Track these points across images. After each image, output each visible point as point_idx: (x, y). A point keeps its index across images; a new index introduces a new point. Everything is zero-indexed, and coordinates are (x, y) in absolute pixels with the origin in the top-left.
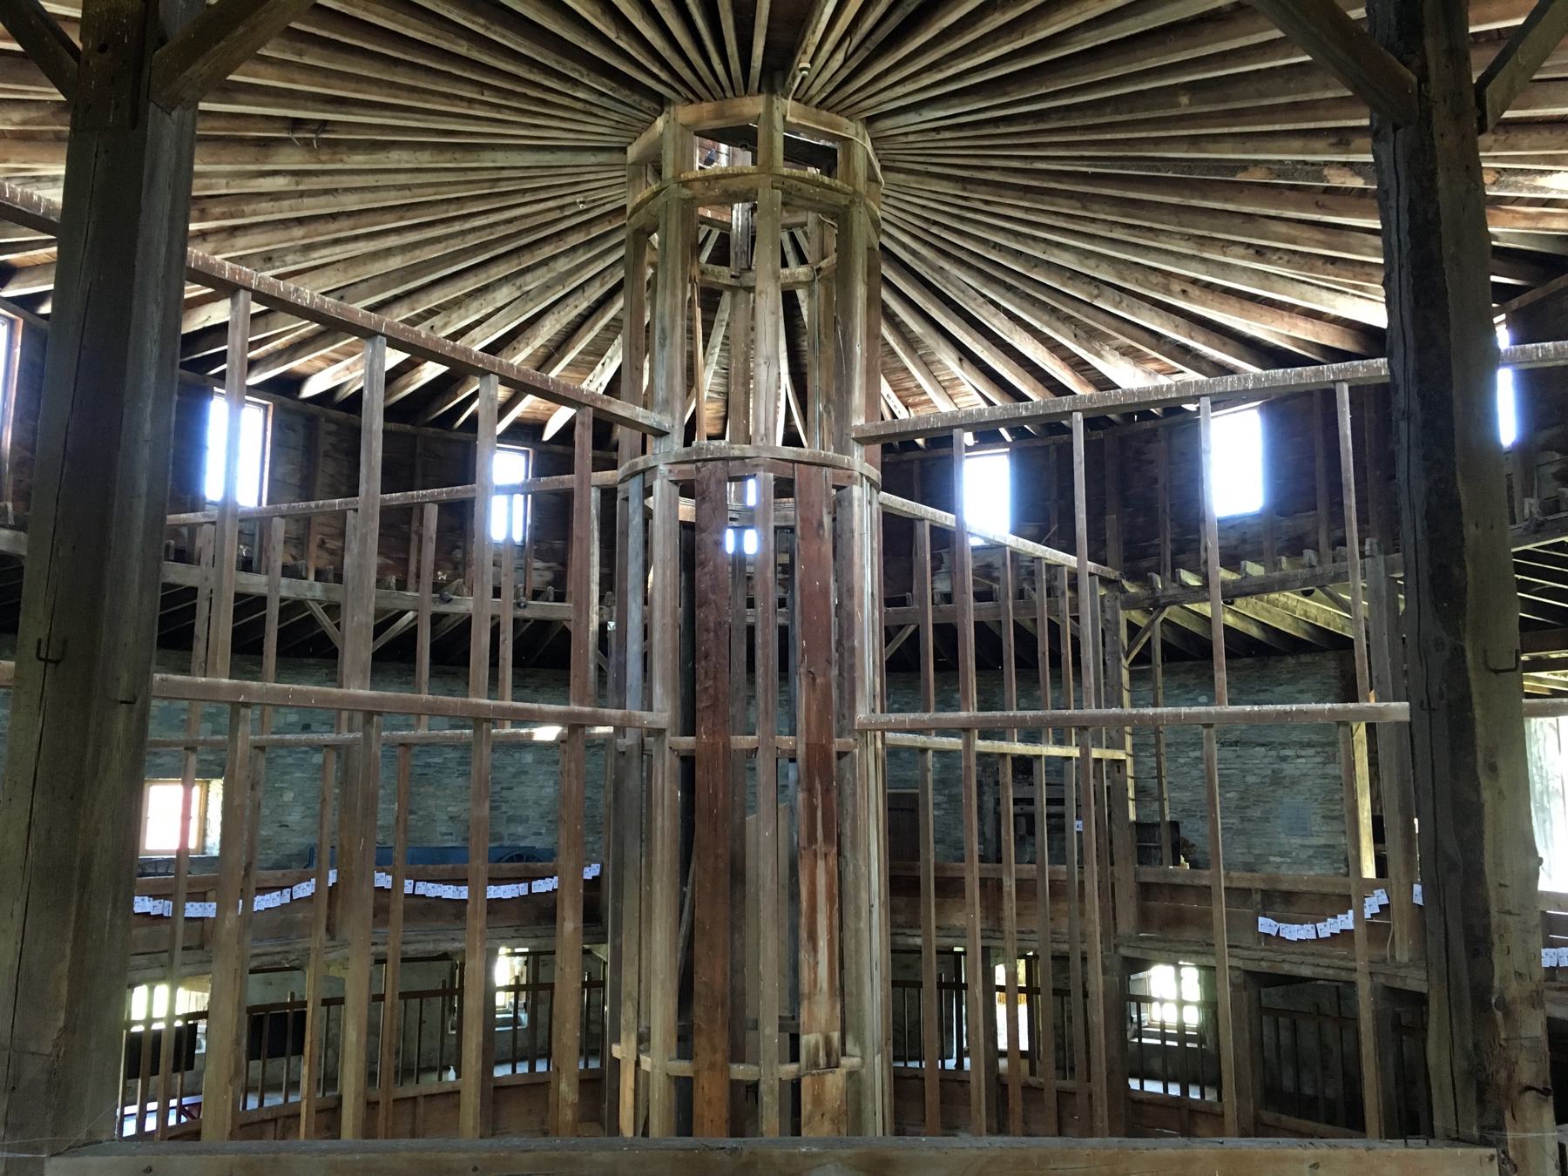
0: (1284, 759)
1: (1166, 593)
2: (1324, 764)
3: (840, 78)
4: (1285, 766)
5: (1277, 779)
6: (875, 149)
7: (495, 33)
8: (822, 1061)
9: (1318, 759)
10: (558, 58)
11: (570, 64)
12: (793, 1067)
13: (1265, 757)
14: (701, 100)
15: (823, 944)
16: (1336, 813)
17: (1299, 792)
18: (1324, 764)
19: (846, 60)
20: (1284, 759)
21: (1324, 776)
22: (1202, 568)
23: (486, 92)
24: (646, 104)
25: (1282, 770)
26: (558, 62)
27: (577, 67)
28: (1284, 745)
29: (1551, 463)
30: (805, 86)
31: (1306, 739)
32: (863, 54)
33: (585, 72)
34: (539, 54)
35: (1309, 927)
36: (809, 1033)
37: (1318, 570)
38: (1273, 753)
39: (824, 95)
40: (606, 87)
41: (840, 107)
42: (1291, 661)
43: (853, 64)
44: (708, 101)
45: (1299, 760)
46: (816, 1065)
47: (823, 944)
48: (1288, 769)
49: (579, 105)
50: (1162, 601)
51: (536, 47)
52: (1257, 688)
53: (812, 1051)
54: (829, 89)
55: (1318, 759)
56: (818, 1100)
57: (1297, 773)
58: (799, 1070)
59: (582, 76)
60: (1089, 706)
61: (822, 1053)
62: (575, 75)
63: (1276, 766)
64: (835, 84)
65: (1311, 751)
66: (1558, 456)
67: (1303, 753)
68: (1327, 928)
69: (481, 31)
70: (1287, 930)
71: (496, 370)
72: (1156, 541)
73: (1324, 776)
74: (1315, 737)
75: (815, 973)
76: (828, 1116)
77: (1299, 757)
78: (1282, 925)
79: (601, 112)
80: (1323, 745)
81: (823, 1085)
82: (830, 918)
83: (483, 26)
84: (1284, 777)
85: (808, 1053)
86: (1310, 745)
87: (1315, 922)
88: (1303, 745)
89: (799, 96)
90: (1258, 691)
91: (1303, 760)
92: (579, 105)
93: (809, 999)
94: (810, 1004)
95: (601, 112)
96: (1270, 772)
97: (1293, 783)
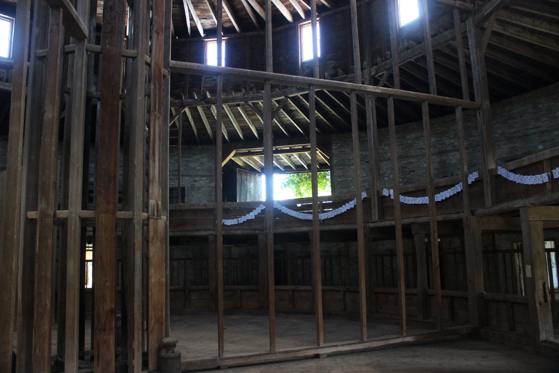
0: (195, 181)
1: (187, 101)
2: (209, 183)
4: (196, 183)
5: (193, 188)
8: (156, 214)
9: (209, 181)
12: (146, 214)
13: (189, 180)
15: (157, 159)
16: (212, 199)
17: (200, 192)
18: (209, 183)
20: (195, 181)
21: (209, 187)
22: (202, 93)
25: (194, 185)
28: (196, 176)
29: (331, 64)
31: (203, 174)
35: (235, 220)
36: (152, 199)
37: (246, 96)
38: (192, 179)
42: (200, 147)
45: (201, 181)
46: (154, 215)
47: (157, 159)
48: (197, 184)
50: (186, 104)
52: (187, 156)
53: (153, 208)
55: (207, 181)
56: (156, 231)
57: (200, 186)
58: (148, 216)
60: (271, 72)
61: (156, 211)
63: (193, 183)
65: (205, 178)
66: (333, 62)
67: (203, 179)
68: (242, 219)
70: (227, 222)
72: (183, 83)
73: (209, 187)
74: (206, 174)
75: (154, 172)
76: (159, 239)
77: (201, 180)
78: (225, 220)
80: (209, 176)
81: (157, 225)
82: (159, 148)
84: (195, 188)
85: (151, 208)
86: (205, 176)
87: (237, 218)
88: (202, 176)
90: (188, 157)
91: (202, 181)
93: (152, 183)
94: (152, 185)
96: (190, 186)
97: (198, 189)
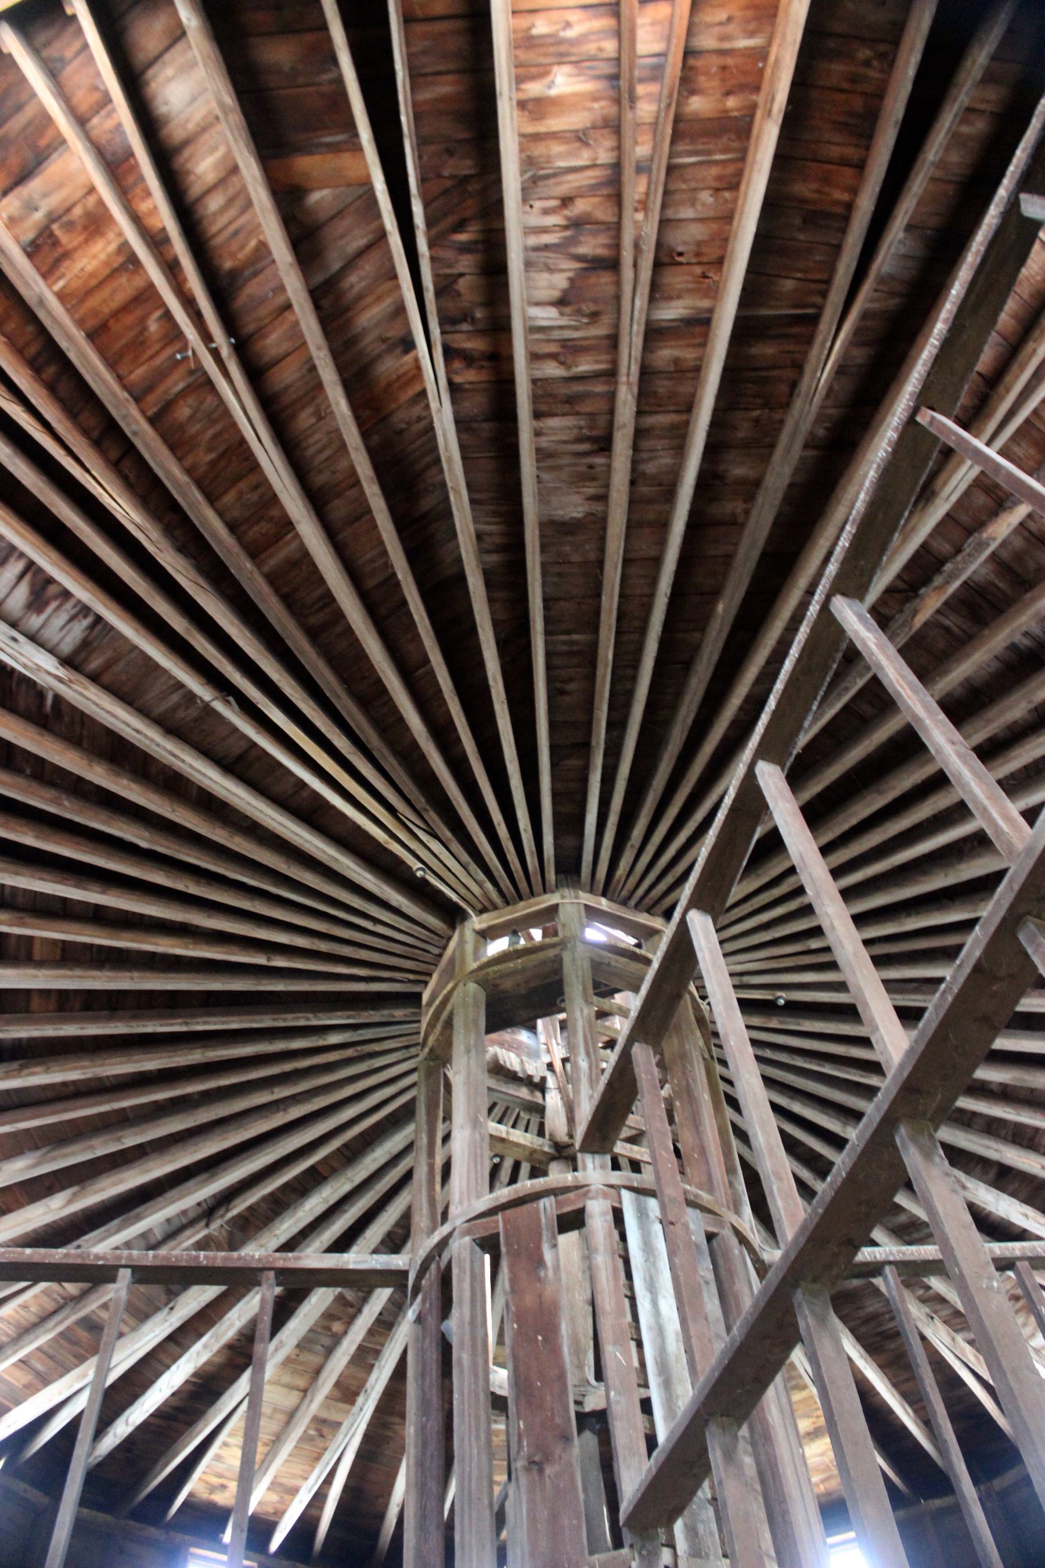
3: (465, 857)
6: (624, 903)
7: (197, 1023)
10: (275, 1017)
11: (290, 1016)
14: (430, 975)
19: (435, 836)
23: (276, 1090)
24: (399, 1014)
26: (274, 1020)
27: (300, 1015)
30: (463, 891)
32: (432, 817)
33: (310, 1015)
34: (250, 1021)
39: (488, 885)
40: (342, 1018)
41: (523, 885)
43: (446, 834)
44: (434, 971)
49: (350, 1053)
51: (244, 1018)
54: (481, 876)
59: (308, 1019)
62: (302, 1023)
64: (473, 867)
69: (184, 1029)
71: (123, 1262)
79: (376, 1047)
83: (181, 1024)
89: (479, 906)
92: (350, 1053)
95: (376, 1047)
